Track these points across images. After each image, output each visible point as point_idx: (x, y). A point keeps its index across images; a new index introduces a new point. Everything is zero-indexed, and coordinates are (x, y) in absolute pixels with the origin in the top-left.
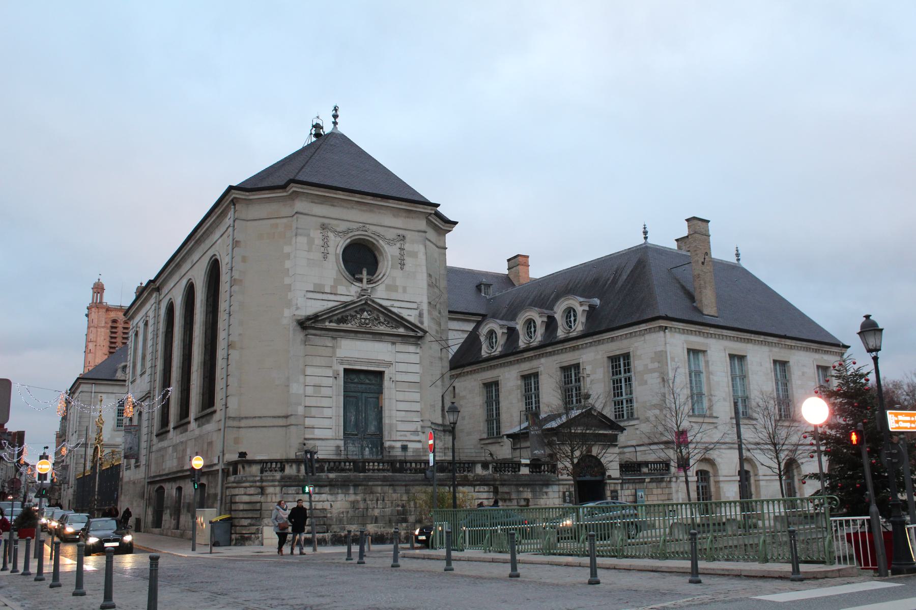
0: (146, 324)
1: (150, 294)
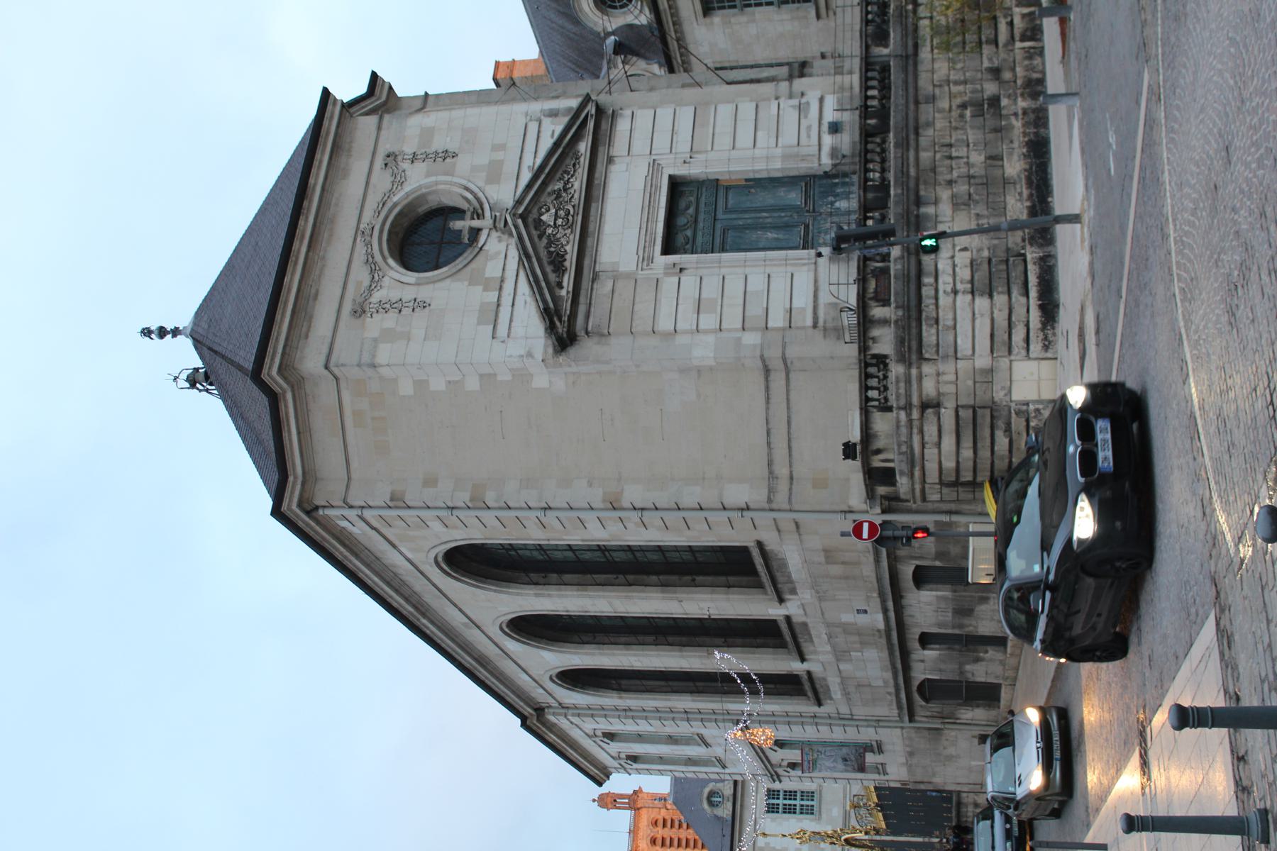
0: (610, 736)
1: (552, 727)
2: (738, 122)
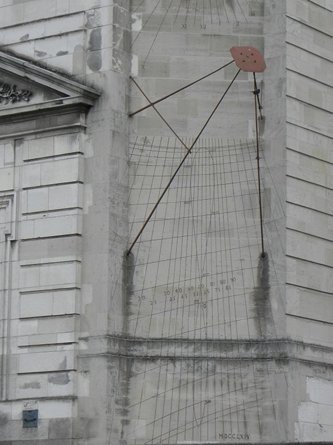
2: (50, 294)
